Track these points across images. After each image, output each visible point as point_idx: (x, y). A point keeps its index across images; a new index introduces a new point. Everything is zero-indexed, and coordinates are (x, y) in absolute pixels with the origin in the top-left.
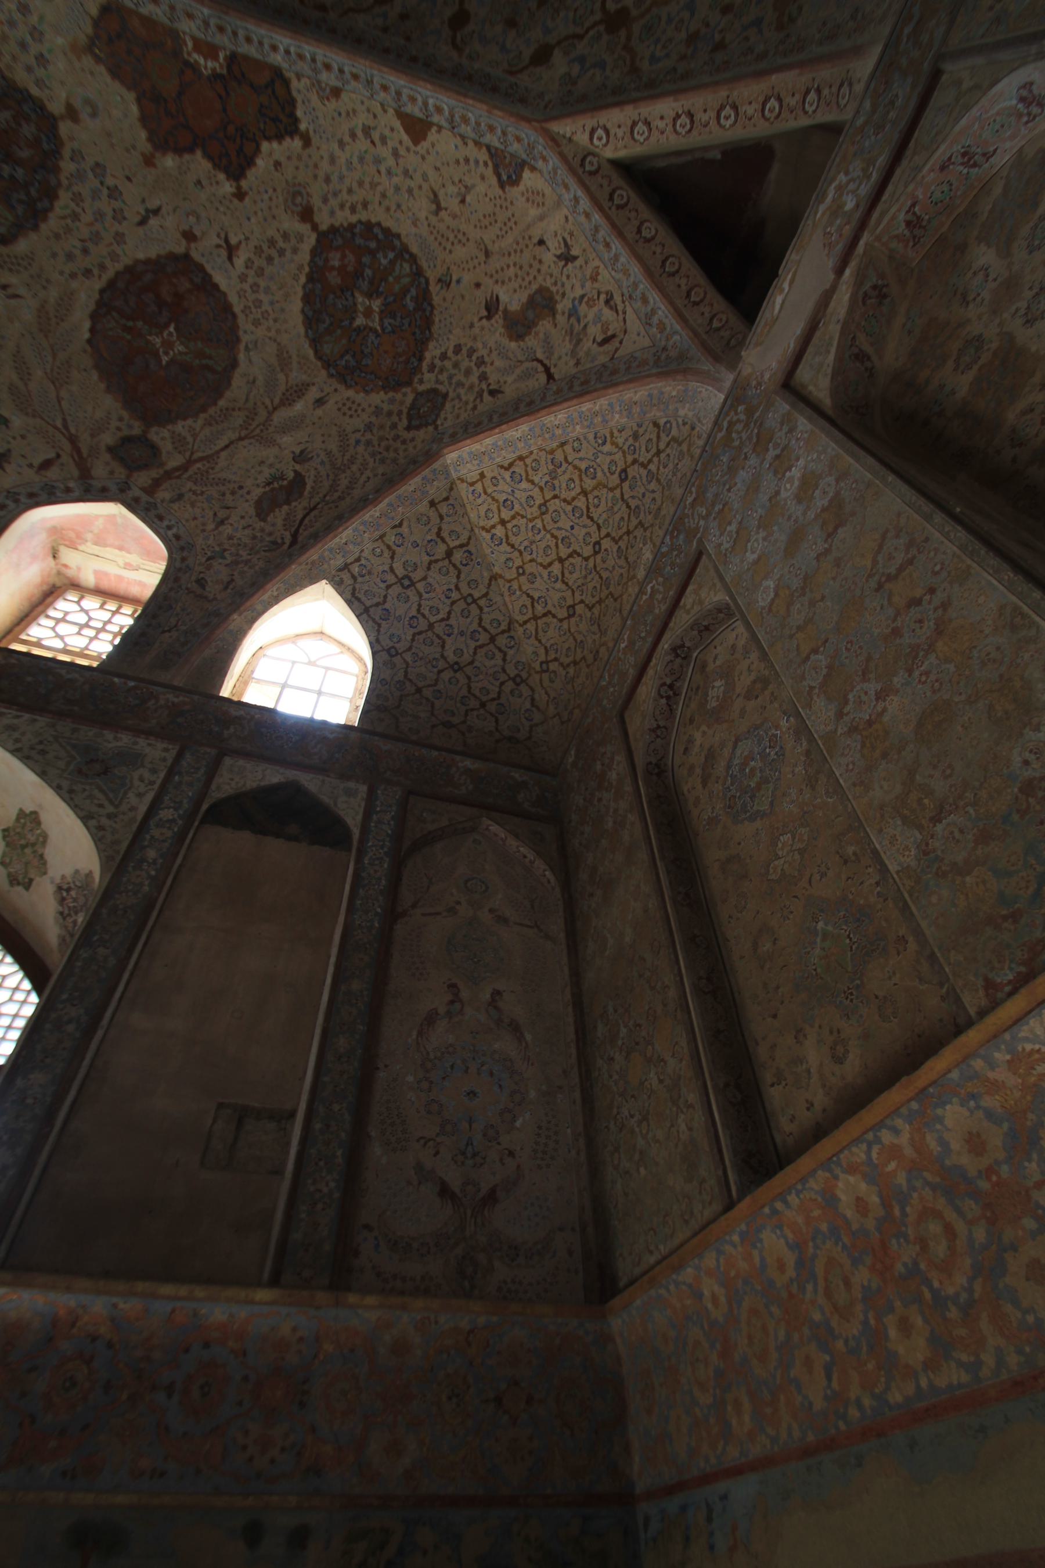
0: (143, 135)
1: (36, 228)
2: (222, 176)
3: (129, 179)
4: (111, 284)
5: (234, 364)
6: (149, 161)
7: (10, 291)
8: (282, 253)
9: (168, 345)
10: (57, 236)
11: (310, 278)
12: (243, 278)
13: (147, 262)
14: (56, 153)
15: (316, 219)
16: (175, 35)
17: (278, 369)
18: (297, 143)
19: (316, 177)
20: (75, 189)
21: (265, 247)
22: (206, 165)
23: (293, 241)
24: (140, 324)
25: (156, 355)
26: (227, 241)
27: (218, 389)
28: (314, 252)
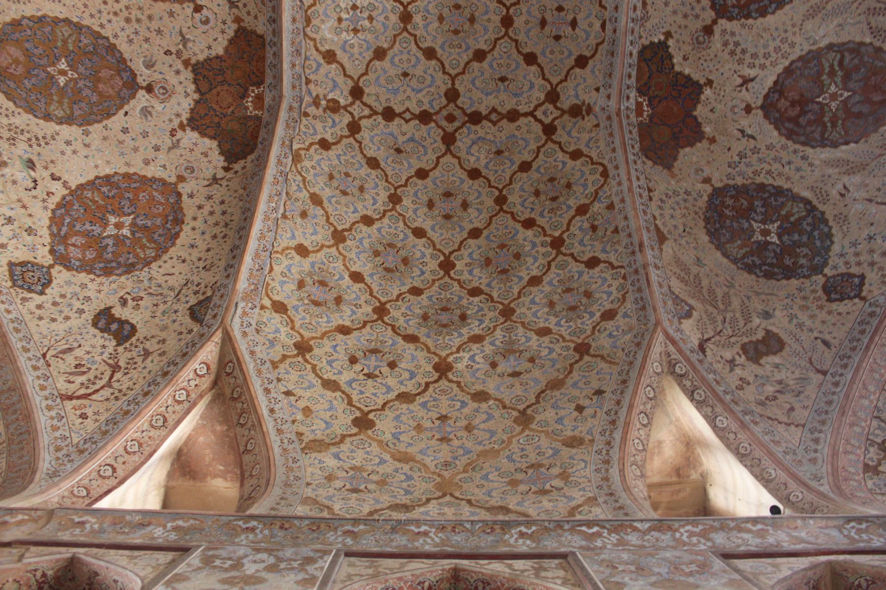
0: (699, 145)
1: (787, 190)
2: (703, 97)
3: (729, 149)
4: (804, 144)
5: (830, 47)
6: (712, 140)
7: (843, 192)
8: (737, 44)
9: (834, 97)
10: (788, 179)
11: (748, 16)
12: (763, 67)
13: (777, 128)
14: (735, 187)
15: (709, 22)
16: (640, 124)
17: (824, 12)
18: (671, 42)
19: (686, 27)
20: (751, 175)
21: (737, 58)
22: (699, 107)
23: (727, 37)
24: (826, 119)
25: (845, 102)
26: (742, 85)
27: (856, 48)
28: (730, 19)
